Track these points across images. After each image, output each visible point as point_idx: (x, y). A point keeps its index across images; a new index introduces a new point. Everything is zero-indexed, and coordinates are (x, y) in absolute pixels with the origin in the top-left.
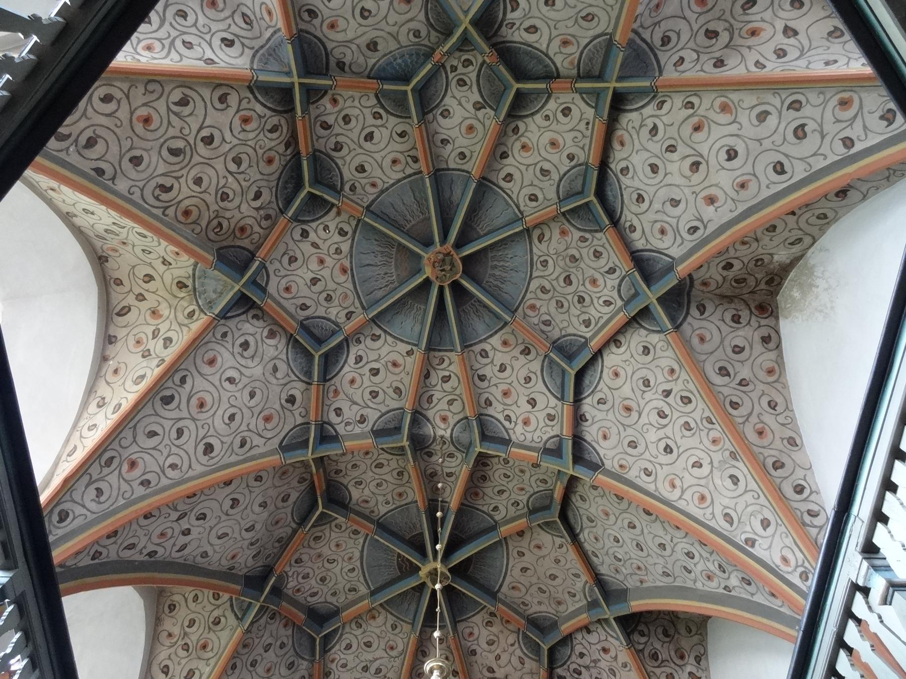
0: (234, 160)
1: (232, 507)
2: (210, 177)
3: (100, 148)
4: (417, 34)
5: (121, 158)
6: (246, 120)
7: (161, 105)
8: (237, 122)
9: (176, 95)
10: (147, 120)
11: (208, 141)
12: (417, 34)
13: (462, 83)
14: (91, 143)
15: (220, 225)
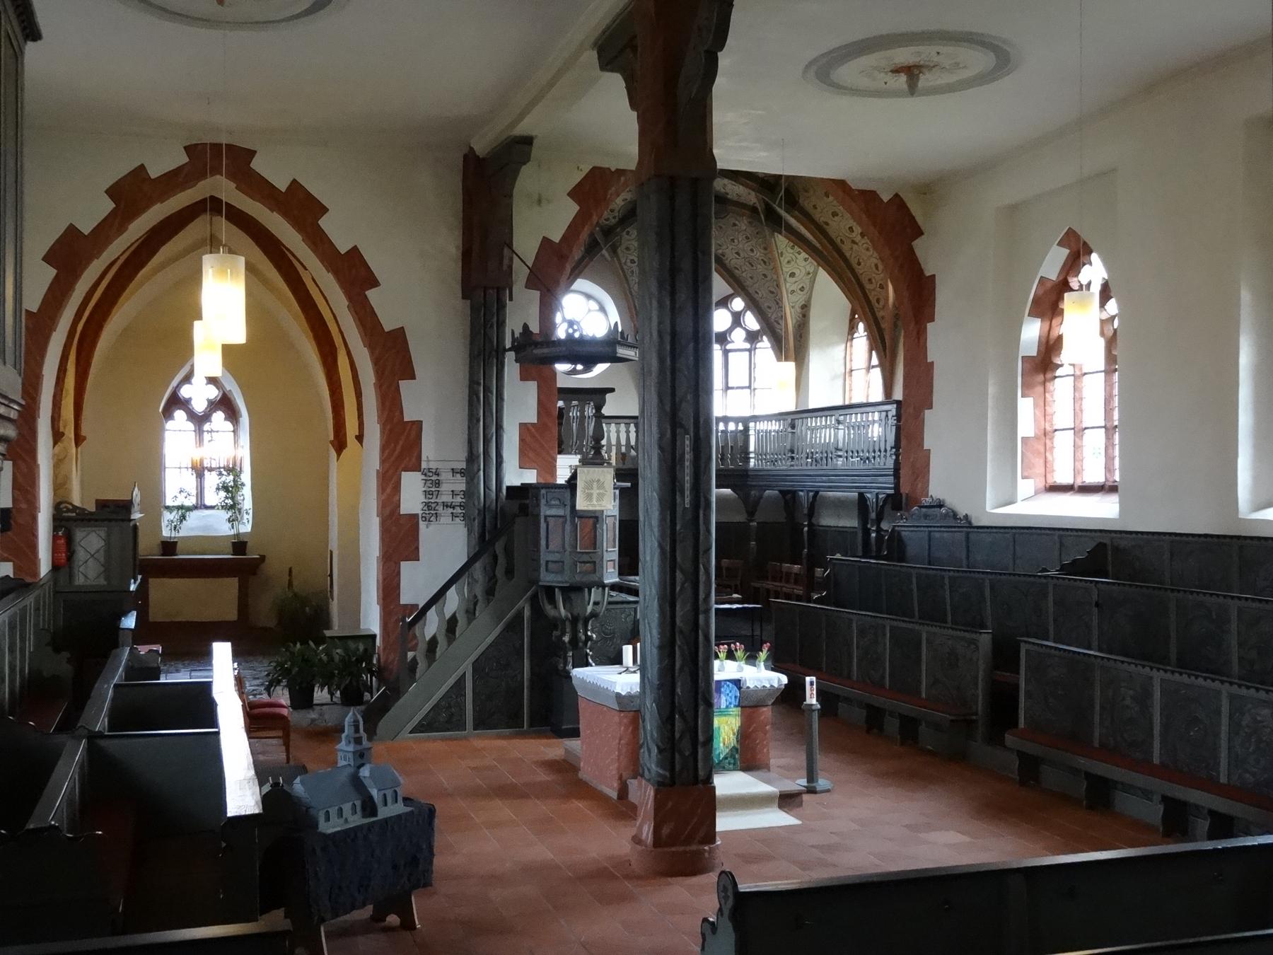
0: (734, 242)
1: (837, 215)
2: (747, 247)
3: (773, 290)
4: (628, 233)
5: (767, 281)
6: (720, 246)
7: (744, 274)
8: (725, 247)
9: (737, 271)
10: (751, 278)
11: (738, 253)
12: (628, 233)
13: (612, 211)
14: (772, 292)
15: (757, 233)
